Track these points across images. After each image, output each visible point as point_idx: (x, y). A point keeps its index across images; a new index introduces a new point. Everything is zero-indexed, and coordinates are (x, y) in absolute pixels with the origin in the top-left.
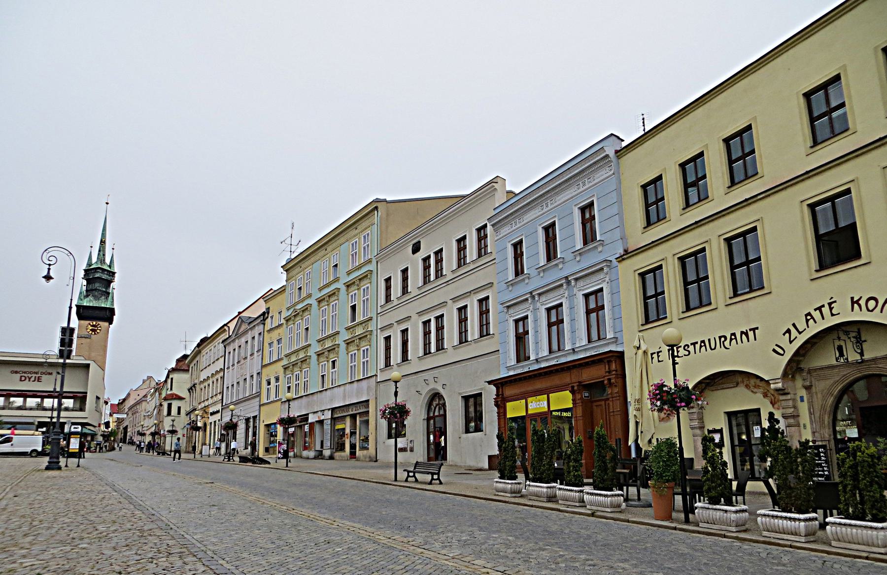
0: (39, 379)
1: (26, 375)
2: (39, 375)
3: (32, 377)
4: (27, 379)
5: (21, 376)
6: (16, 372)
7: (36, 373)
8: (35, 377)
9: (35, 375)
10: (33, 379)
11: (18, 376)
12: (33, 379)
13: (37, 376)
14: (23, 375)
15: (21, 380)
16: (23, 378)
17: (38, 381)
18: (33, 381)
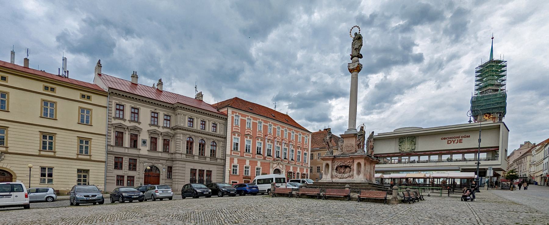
0: (460, 141)
1: (451, 140)
2: (460, 139)
3: (455, 140)
4: (452, 142)
5: (448, 141)
6: (445, 139)
7: (459, 137)
8: (458, 140)
9: (458, 139)
10: (456, 141)
11: (446, 140)
12: (456, 141)
13: (459, 139)
14: (450, 139)
15: (448, 143)
16: (449, 142)
17: (460, 143)
18: (456, 143)
